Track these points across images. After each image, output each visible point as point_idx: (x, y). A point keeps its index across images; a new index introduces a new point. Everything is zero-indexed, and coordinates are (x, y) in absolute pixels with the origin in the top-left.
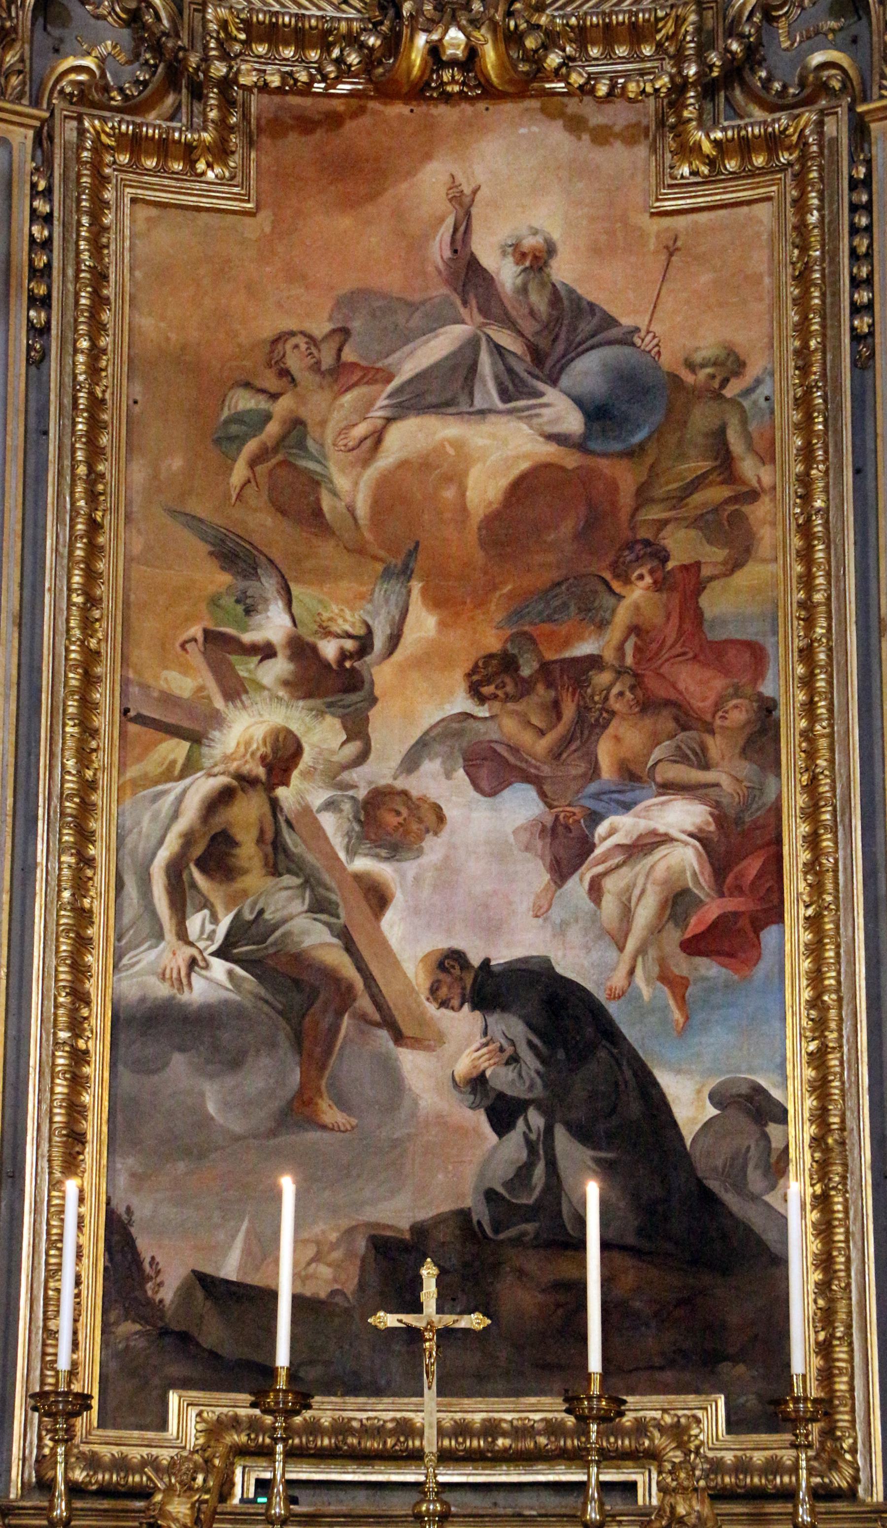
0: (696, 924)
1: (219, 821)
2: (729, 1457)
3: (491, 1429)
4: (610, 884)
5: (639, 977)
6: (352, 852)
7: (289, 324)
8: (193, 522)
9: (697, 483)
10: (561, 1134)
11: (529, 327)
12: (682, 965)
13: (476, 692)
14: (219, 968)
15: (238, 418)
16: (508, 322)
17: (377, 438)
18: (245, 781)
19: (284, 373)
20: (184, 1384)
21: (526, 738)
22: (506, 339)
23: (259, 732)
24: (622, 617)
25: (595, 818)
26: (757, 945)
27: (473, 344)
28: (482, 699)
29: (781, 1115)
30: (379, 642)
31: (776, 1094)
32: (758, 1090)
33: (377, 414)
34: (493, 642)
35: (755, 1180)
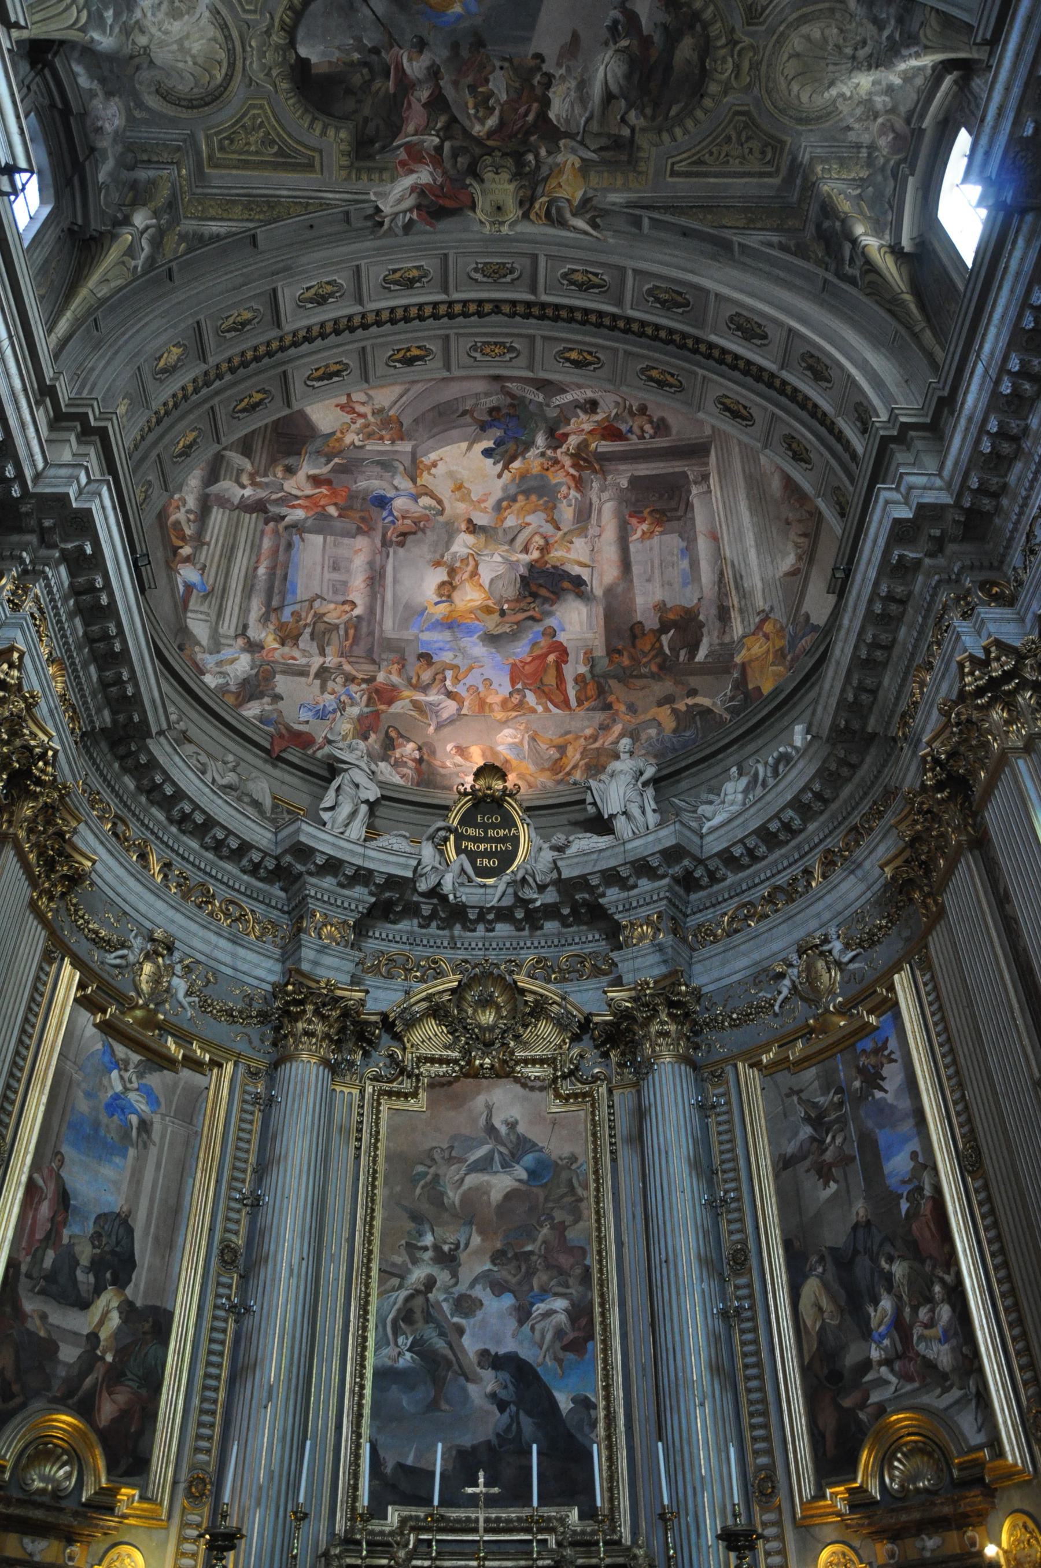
0: (566, 1340)
1: (409, 1305)
2: (579, 1529)
3: (498, 1520)
4: (538, 1327)
5: (547, 1359)
6: (452, 1316)
7: (434, 1144)
8: (405, 1208)
9: (562, 1197)
10: (522, 1413)
11: (510, 1146)
12: (561, 1354)
13: (493, 1262)
14: (408, 1355)
15: (418, 1174)
16: (504, 1145)
17: (462, 1180)
18: (418, 1292)
19: (433, 1160)
20: (393, 1503)
21: (509, 1277)
22: (503, 1149)
23: (423, 1275)
24: (540, 1238)
25: (532, 1304)
26: (585, 1349)
27: (492, 1152)
28: (495, 1265)
29: (595, 1407)
30: (462, 1246)
31: (593, 1399)
32: (587, 1398)
33: (462, 1172)
34: (498, 1245)
35: (586, 1429)
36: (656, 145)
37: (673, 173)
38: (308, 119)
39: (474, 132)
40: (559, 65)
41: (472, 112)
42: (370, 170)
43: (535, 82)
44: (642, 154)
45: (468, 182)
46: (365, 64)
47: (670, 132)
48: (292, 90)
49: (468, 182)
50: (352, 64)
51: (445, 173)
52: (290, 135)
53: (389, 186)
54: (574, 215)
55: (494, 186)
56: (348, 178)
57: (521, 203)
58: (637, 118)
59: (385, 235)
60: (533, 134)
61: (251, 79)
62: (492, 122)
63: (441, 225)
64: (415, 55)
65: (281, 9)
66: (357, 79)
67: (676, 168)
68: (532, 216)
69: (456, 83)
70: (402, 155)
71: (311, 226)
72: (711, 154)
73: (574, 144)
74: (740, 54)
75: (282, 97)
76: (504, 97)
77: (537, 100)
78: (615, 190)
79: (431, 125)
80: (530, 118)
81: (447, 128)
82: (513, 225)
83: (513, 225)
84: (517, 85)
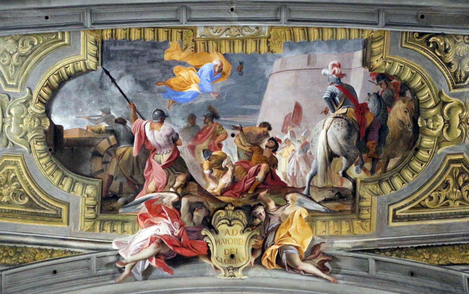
36: (378, 195)
37: (396, 218)
38: (58, 176)
39: (209, 190)
40: (284, 131)
41: (207, 172)
42: (113, 222)
43: (263, 146)
44: (364, 203)
45: (203, 233)
46: (112, 132)
47: (390, 181)
48: (45, 151)
49: (203, 233)
50: (100, 132)
51: (181, 226)
52: (41, 190)
53: (131, 237)
54: (303, 260)
55: (227, 236)
56: (92, 229)
57: (253, 251)
58: (357, 171)
59: (124, 280)
60: (264, 189)
61: (8, 140)
62: (225, 180)
63: (178, 271)
64: (156, 126)
65: (40, 86)
66: (104, 145)
67: (398, 213)
68: (264, 262)
69: (192, 148)
70: (143, 209)
71: (55, 272)
72: (431, 198)
73: (298, 197)
74: (449, 112)
75: (35, 157)
76: (235, 159)
77: (266, 161)
78: (343, 237)
79: (170, 183)
80: (260, 176)
81: (184, 186)
82: (246, 269)
83: (246, 269)
84: (247, 149)
